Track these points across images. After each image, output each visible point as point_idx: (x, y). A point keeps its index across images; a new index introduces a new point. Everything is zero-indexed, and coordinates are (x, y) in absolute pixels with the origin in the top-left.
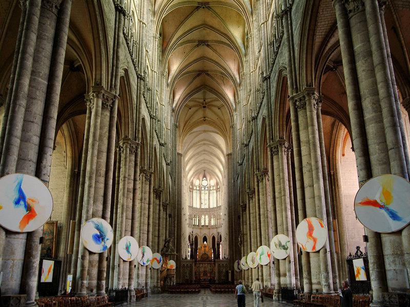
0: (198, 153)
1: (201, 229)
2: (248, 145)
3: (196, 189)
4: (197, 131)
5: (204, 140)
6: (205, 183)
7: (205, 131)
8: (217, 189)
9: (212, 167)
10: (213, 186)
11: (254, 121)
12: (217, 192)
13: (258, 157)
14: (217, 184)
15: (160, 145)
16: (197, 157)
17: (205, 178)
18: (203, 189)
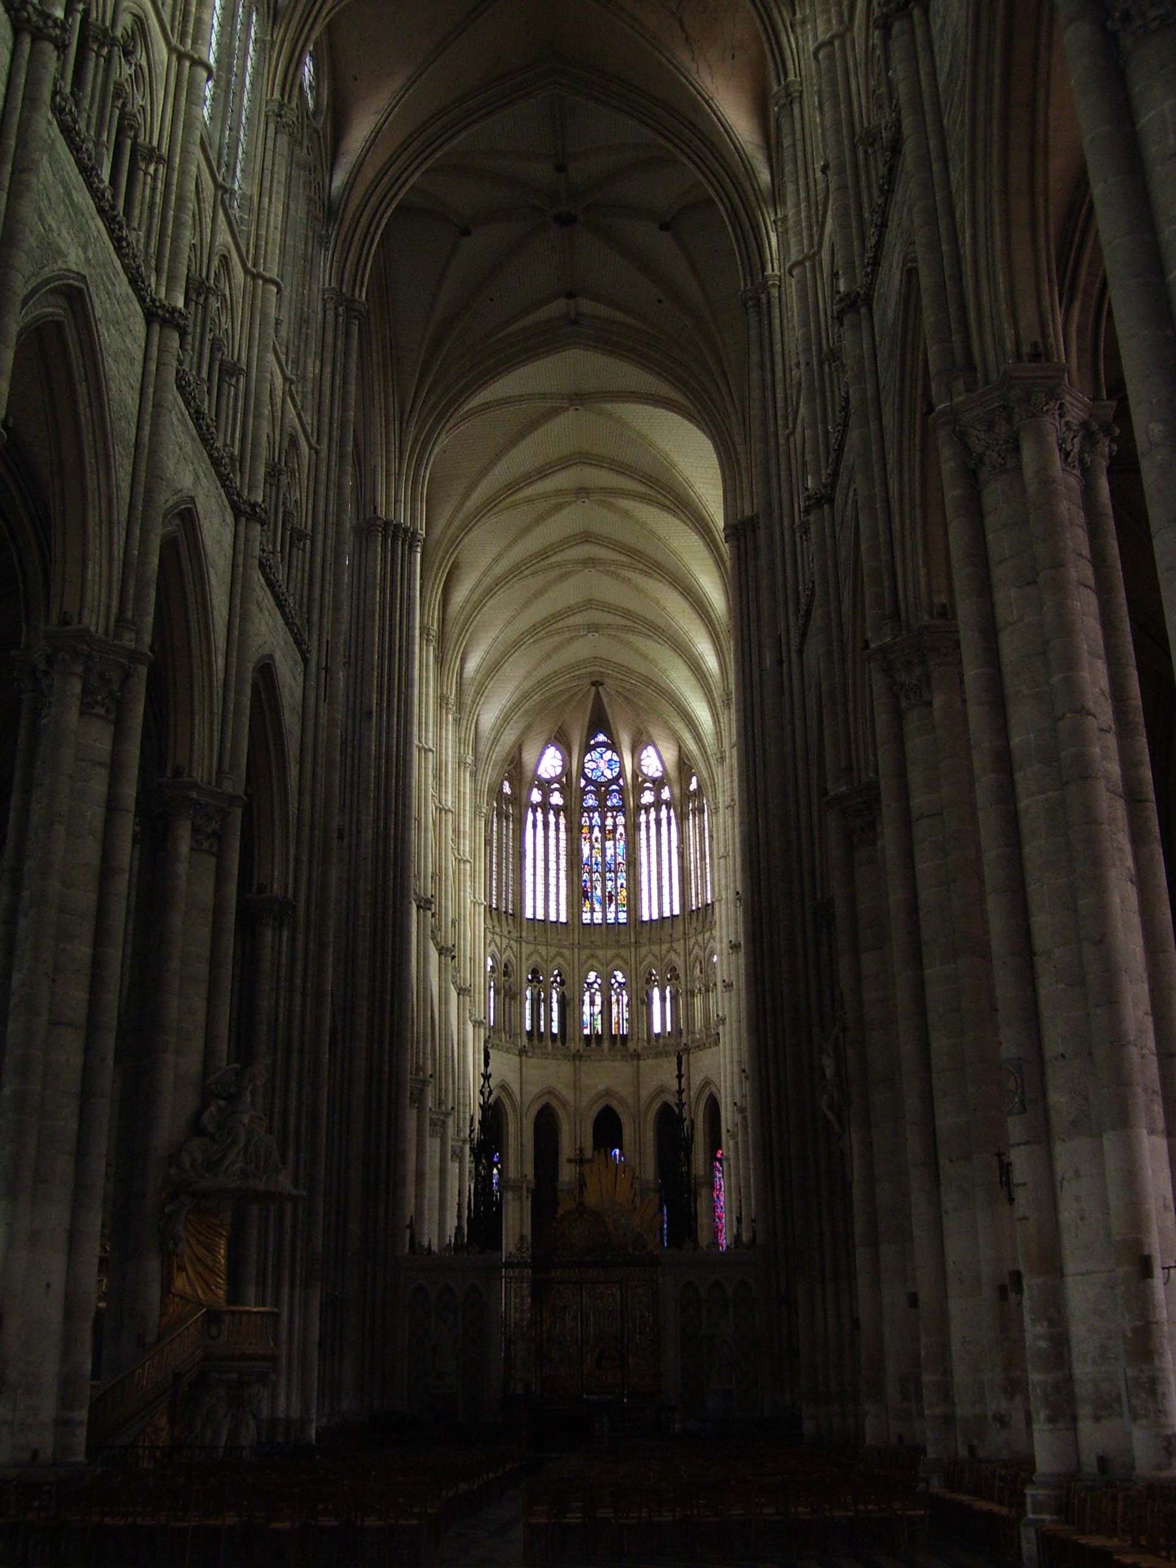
0: (543, 554)
1: (577, 1057)
2: (869, 301)
3: (545, 806)
4: (521, 398)
5: (583, 458)
6: (600, 764)
7: (579, 399)
8: (686, 796)
9: (644, 657)
10: (658, 784)
11: (896, 28)
12: (682, 819)
13: (959, 277)
14: (685, 767)
15: (150, 317)
16: (535, 583)
17: (601, 738)
18: (590, 801)
